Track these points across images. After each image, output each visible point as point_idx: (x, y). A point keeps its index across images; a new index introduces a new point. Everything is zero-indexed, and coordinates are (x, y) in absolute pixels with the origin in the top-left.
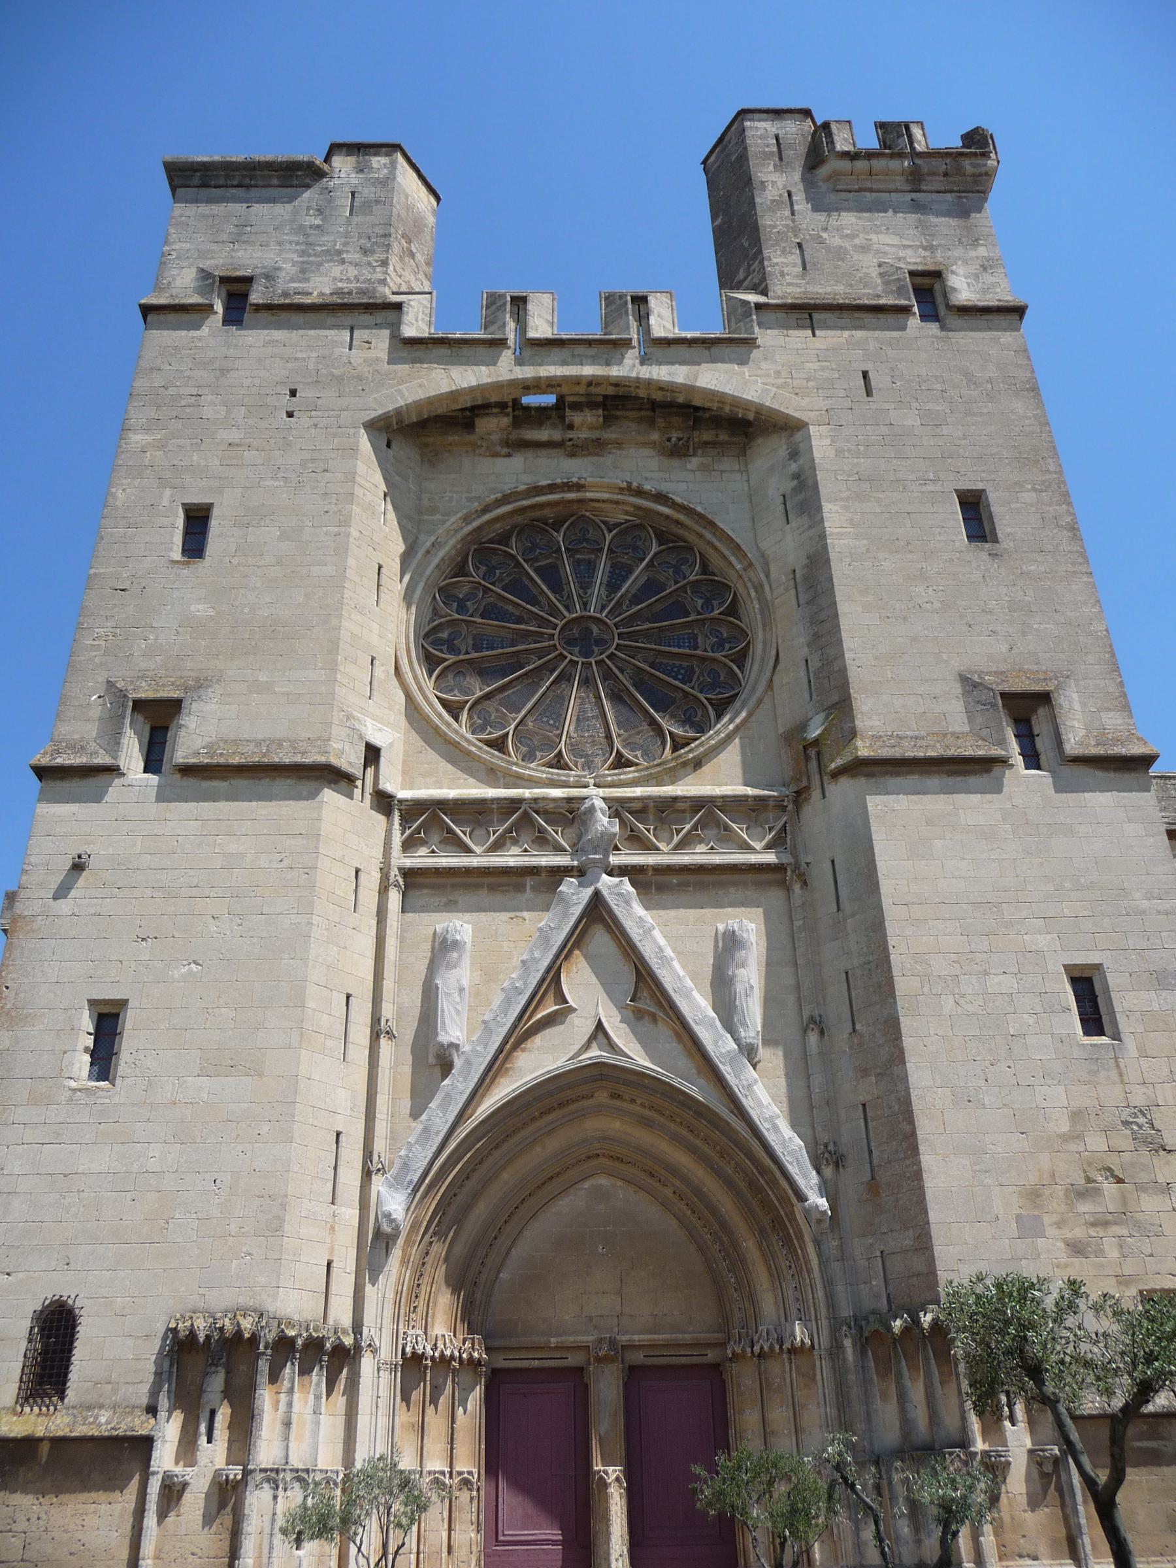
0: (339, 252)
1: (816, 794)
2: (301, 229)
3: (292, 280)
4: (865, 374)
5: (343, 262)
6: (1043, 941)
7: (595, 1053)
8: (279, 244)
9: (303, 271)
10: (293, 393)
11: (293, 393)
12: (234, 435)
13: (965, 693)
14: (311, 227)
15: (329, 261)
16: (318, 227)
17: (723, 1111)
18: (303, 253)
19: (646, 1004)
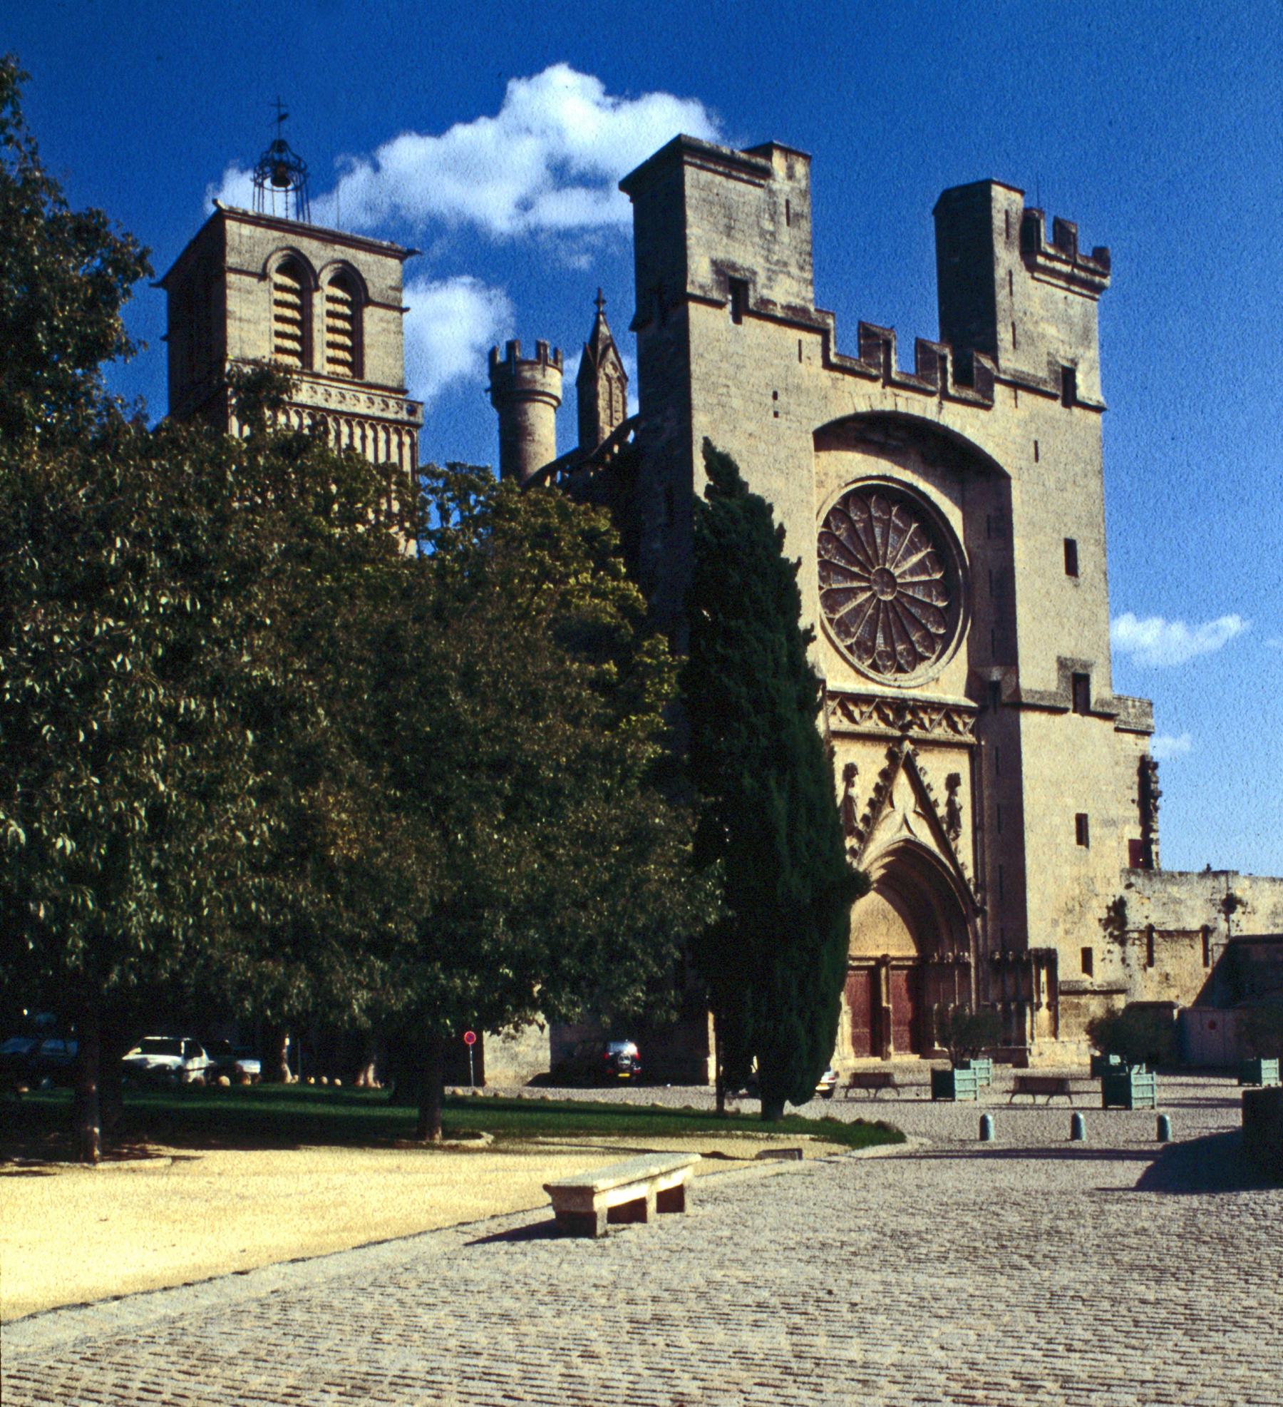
0: (785, 264)
1: (991, 710)
2: (762, 233)
3: (764, 286)
4: (1036, 443)
5: (789, 274)
6: (1070, 802)
7: (905, 833)
8: (753, 244)
9: (770, 279)
10: (775, 396)
11: (775, 396)
12: (751, 427)
13: (1059, 669)
14: (768, 232)
15: (781, 272)
16: (772, 234)
17: (947, 863)
18: (767, 260)
19: (919, 810)
